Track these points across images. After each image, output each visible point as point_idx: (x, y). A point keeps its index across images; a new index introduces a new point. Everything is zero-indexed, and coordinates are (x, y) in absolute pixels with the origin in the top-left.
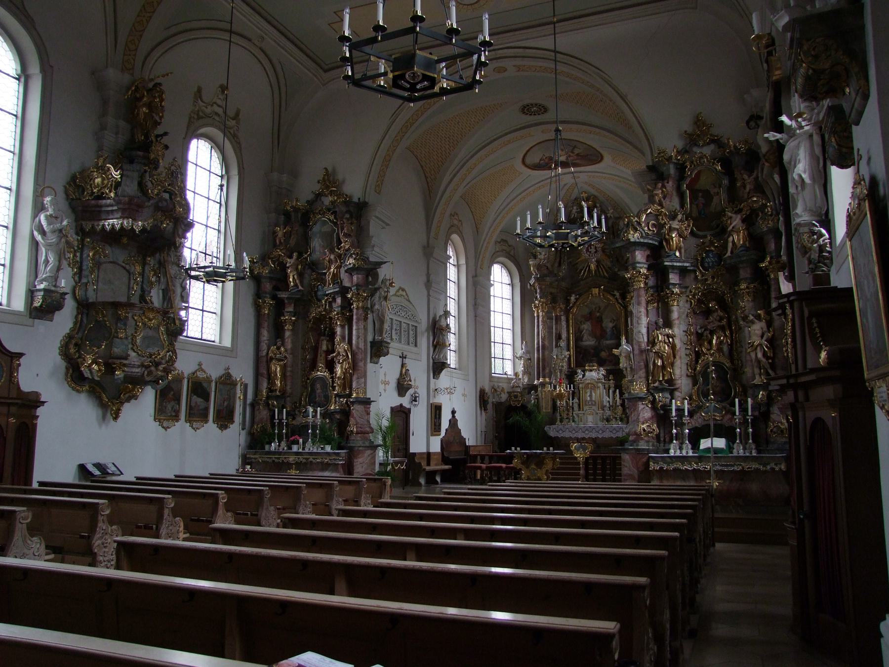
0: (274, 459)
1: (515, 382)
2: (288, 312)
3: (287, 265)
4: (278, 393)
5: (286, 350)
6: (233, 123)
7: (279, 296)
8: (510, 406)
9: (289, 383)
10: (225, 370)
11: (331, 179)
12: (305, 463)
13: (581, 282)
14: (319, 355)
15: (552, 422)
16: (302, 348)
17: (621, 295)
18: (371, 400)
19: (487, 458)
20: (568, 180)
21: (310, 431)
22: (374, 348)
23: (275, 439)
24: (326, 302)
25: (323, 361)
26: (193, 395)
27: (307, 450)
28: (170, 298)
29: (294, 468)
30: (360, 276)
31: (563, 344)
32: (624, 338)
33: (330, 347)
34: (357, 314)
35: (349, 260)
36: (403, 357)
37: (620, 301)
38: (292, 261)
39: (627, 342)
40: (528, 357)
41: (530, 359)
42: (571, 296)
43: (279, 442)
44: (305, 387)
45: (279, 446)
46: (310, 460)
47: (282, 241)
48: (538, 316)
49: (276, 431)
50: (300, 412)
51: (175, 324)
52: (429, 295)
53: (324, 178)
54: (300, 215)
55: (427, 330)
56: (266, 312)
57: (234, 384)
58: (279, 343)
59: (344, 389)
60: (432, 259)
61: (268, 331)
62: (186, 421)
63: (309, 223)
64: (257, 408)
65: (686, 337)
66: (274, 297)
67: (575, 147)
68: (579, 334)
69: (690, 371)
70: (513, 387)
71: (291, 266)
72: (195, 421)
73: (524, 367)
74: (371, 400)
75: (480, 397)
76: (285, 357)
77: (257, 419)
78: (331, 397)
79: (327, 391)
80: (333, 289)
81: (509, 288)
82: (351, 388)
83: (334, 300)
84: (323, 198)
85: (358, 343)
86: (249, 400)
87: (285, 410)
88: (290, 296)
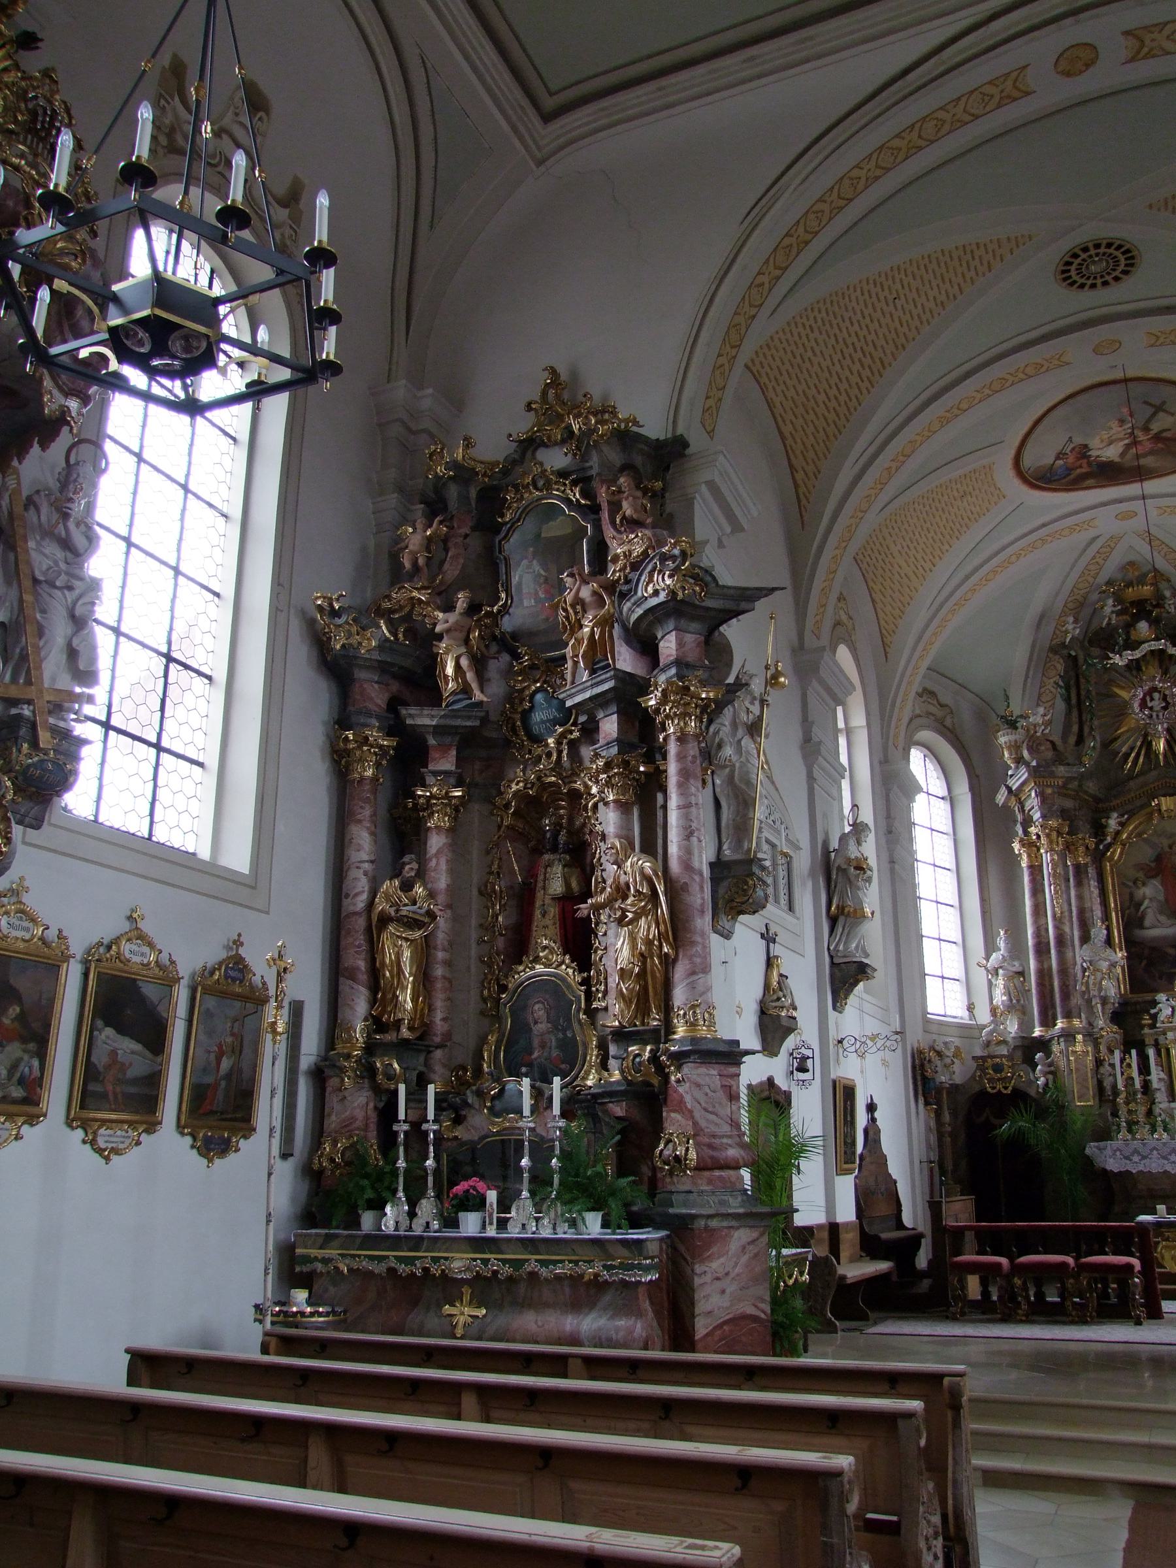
0: (393, 1263)
1: (991, 1032)
2: (435, 773)
3: (438, 629)
4: (405, 1033)
5: (431, 895)
6: (282, 214)
7: (409, 721)
8: (983, 1093)
9: (439, 1003)
10: (228, 948)
11: (566, 396)
12: (510, 1279)
13: (1132, 784)
14: (538, 913)
15: (1104, 1134)
16: (481, 893)
18: (743, 1046)
19: (969, 1236)
20: (1106, 523)
21: (525, 1162)
22: (725, 884)
23: (395, 1191)
24: (559, 743)
25: (554, 930)
26: (100, 1023)
27: (514, 1232)
28: (24, 657)
29: (466, 1298)
30: (689, 638)
31: (1099, 932)
33: (574, 884)
34: (681, 757)
35: (651, 580)
36: (769, 938)
38: (453, 617)
40: (1017, 966)
41: (1021, 974)
42: (1108, 818)
43: (413, 1203)
44: (491, 1013)
45: (412, 1214)
46: (528, 1268)
47: (421, 561)
48: (1036, 870)
49: (401, 1164)
50: (480, 1094)
51: (35, 744)
52: (811, 778)
53: (544, 393)
54: (473, 493)
55: (812, 874)
56: (369, 773)
57: (256, 999)
58: (409, 870)
59: (643, 1010)
60: (815, 683)
61: (372, 834)
62: (69, 1123)
63: (502, 516)
64: (333, 1082)
66: (395, 727)
67: (1159, 409)
68: (1132, 909)
70: (988, 1044)
71: (448, 631)
72: (104, 1122)
73: (1008, 993)
74: (743, 1046)
75: (914, 1067)
76: (431, 915)
77: (332, 1122)
78: (586, 1046)
79: (570, 1026)
80: (592, 686)
81: (944, 807)
82: (667, 1009)
83: (590, 731)
84: (542, 454)
85: (687, 851)
86: (307, 1060)
87: (431, 1088)
88: (443, 722)
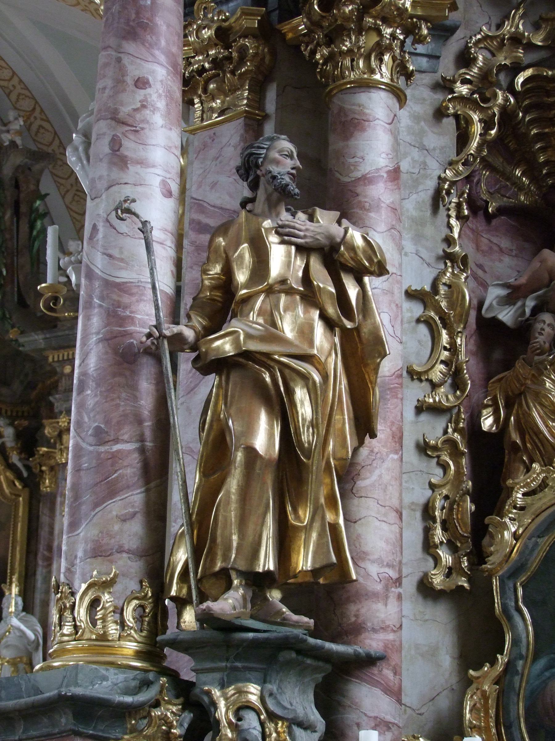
17: (18, 435)
32: (15, 590)
37: (15, 458)
39: (27, 608)
65: (423, 329)
69: (446, 557)
